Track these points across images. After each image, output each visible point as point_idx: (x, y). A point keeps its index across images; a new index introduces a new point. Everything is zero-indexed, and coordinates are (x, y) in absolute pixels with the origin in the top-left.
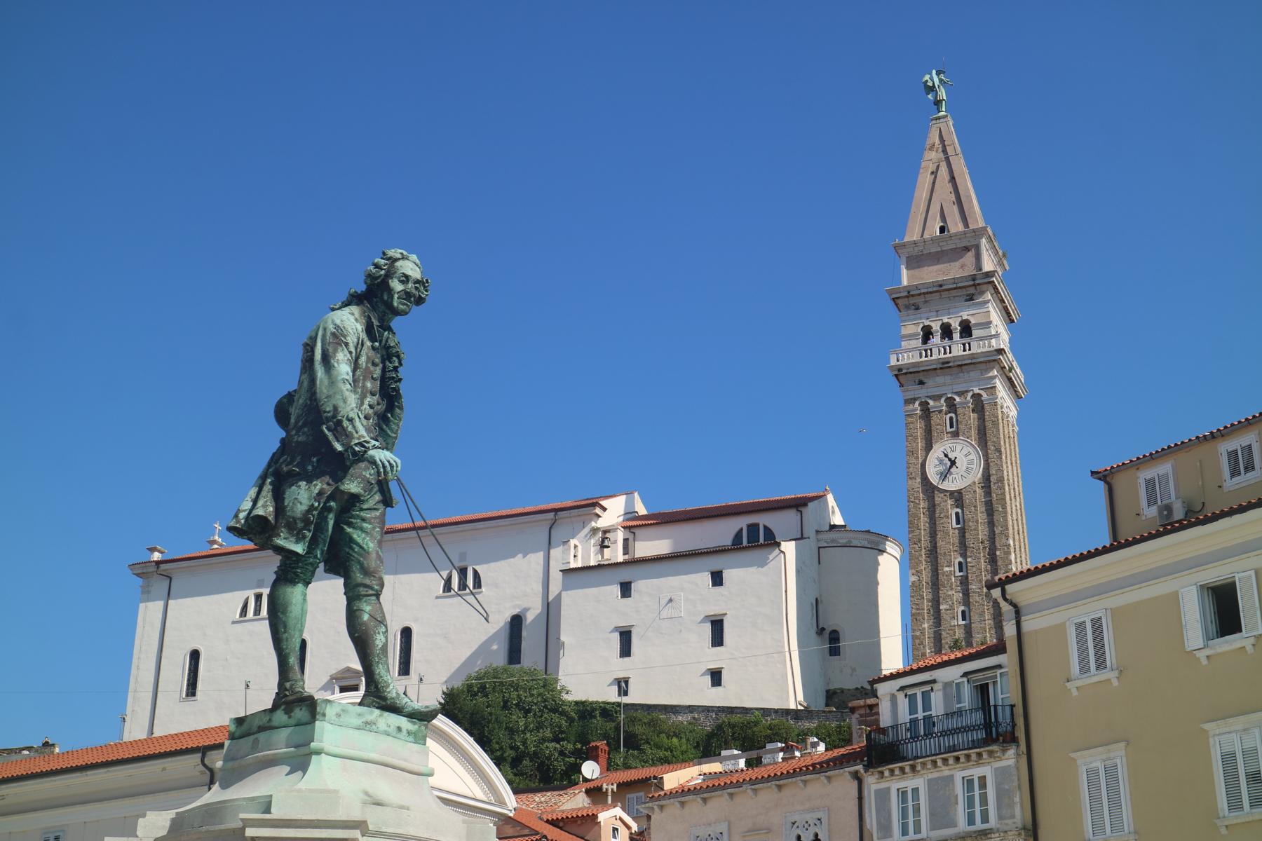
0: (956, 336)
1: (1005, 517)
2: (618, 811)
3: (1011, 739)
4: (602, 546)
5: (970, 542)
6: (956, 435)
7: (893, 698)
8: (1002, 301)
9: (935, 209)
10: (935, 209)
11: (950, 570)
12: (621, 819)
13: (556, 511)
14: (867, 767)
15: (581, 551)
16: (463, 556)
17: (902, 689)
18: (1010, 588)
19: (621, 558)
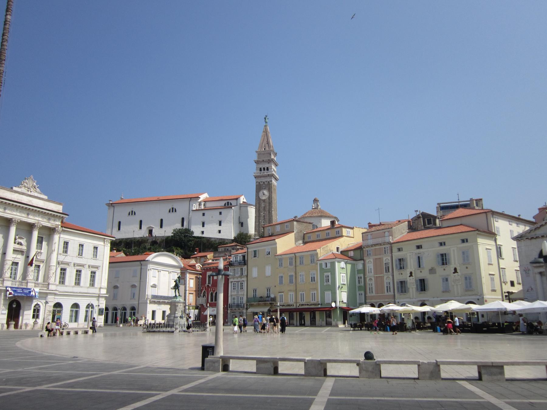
0: (266, 170)
1: (272, 205)
2: (199, 264)
3: (246, 264)
4: (200, 205)
5: (266, 209)
6: (265, 189)
7: (233, 257)
8: (275, 163)
9: (264, 144)
10: (264, 144)
11: (262, 214)
12: (199, 266)
13: (191, 198)
14: (230, 266)
15: (195, 207)
16: (173, 206)
17: (235, 256)
18: (247, 246)
19: (203, 208)
